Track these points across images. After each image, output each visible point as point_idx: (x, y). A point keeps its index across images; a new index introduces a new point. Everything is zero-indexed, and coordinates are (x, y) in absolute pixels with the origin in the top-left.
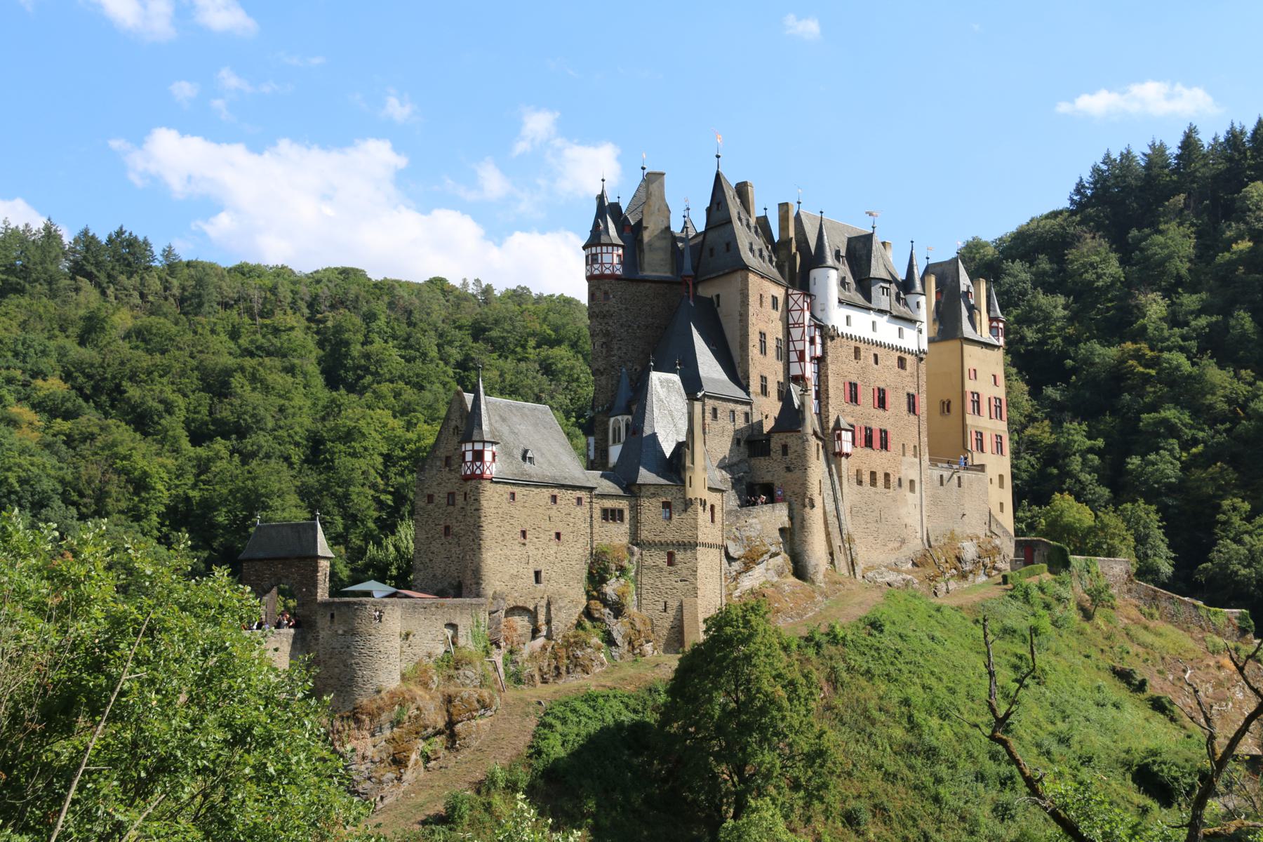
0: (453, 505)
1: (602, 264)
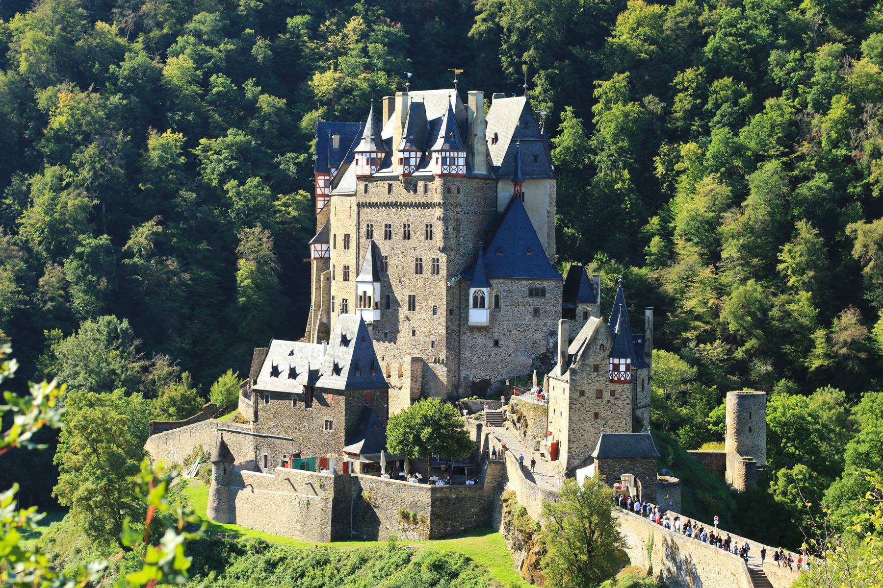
0: (601, 398)
1: (458, 166)
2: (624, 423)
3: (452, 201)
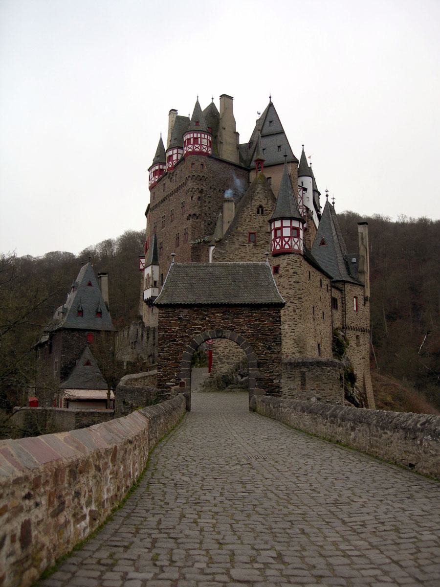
1: (201, 145)
2: (291, 309)
3: (196, 175)
